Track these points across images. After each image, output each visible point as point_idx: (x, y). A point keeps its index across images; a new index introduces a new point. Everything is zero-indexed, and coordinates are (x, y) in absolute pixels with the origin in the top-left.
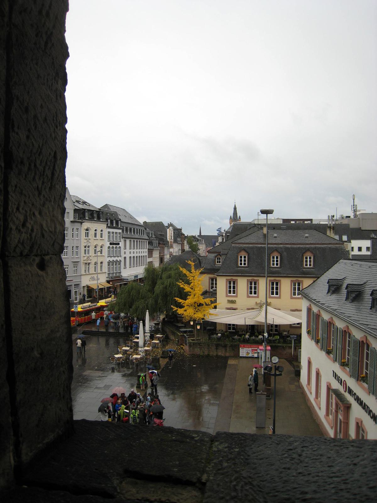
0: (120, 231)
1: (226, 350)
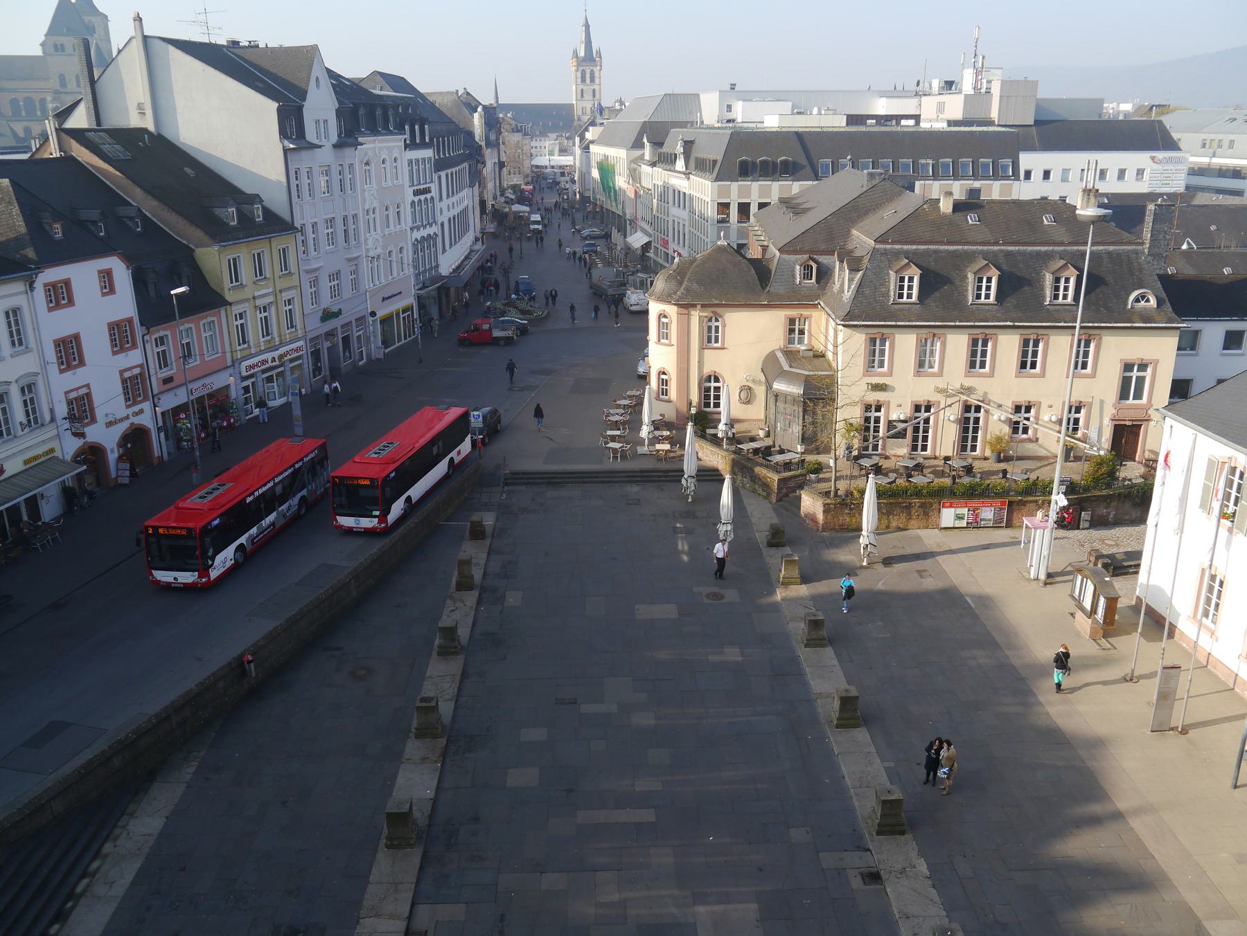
0: (428, 153)
1: (909, 514)
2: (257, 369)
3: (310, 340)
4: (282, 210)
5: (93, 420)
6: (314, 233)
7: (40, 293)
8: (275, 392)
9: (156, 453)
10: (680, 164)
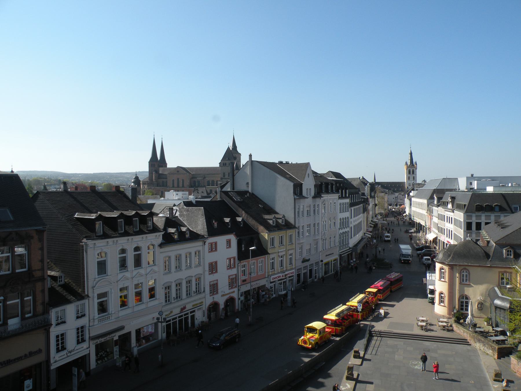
0: (347, 201)
2: (276, 279)
3: (298, 270)
4: (292, 221)
5: (217, 293)
6: (302, 229)
7: (207, 246)
8: (282, 289)
9: (237, 308)
10: (450, 206)
